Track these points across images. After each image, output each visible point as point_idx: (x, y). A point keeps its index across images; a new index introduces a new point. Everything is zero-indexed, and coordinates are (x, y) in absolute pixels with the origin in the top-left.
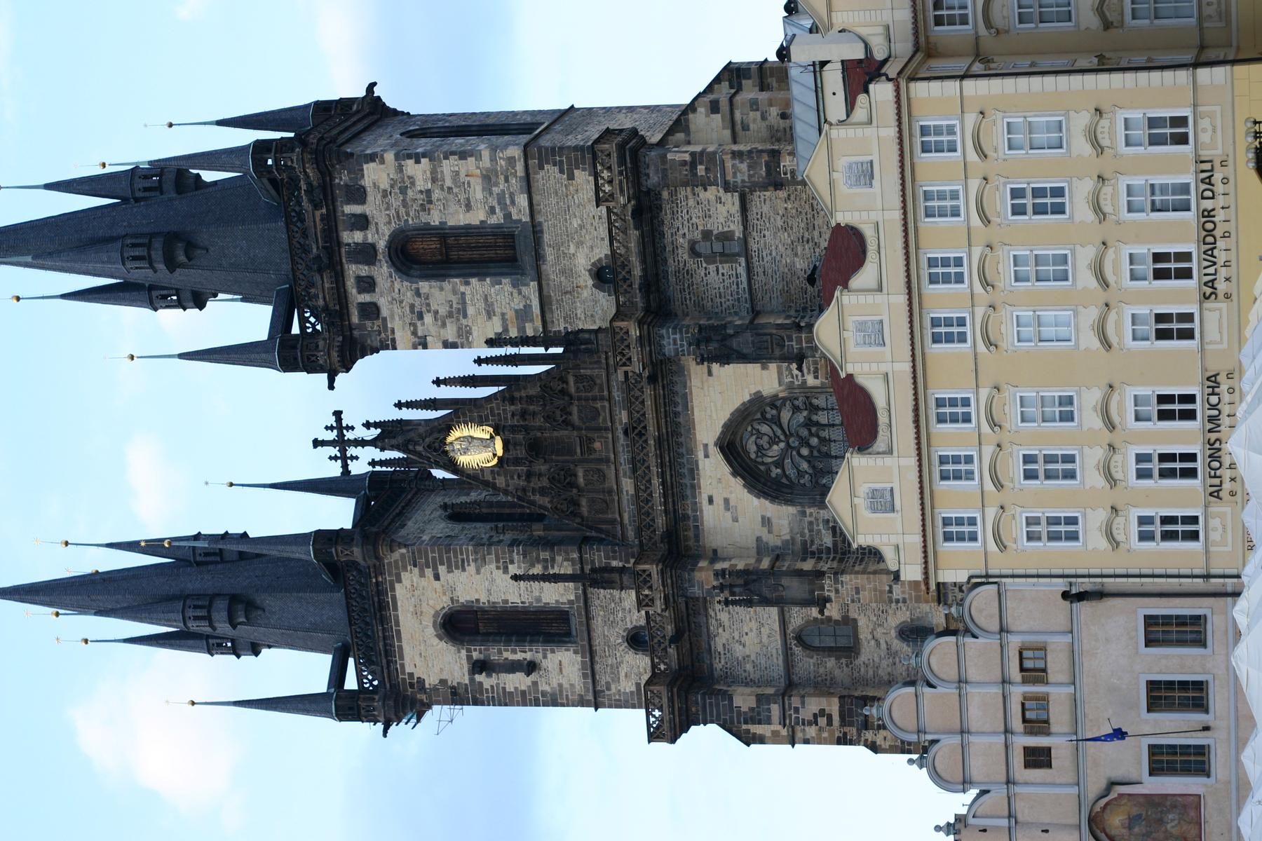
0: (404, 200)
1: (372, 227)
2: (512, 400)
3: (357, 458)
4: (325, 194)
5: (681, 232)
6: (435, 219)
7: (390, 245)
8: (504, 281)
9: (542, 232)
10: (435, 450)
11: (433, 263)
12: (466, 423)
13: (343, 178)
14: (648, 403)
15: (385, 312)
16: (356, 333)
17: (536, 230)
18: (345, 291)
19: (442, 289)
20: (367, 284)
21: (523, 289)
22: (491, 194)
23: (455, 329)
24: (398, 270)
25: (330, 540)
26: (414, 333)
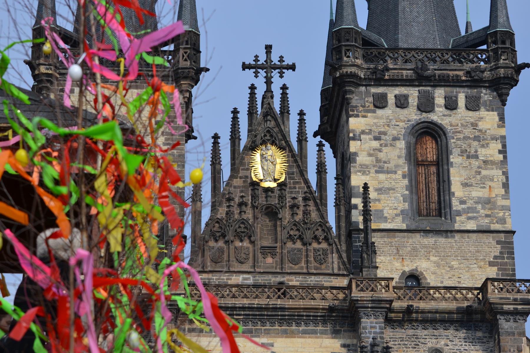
0: (469, 137)
1: (448, 112)
2: (305, 199)
3: (256, 76)
4: (474, 82)
5: (449, 343)
6: (455, 159)
7: (432, 123)
8: (407, 204)
9: (447, 237)
10: (265, 136)
11: (415, 154)
12: (288, 162)
13: (486, 95)
14: (313, 303)
15: (380, 112)
16: (363, 89)
17: (449, 232)
18: (397, 86)
19: (399, 157)
20: (402, 103)
21: (400, 218)
22: (476, 203)
23: (367, 163)
24: (414, 127)
25: (195, 44)
26: (363, 132)
